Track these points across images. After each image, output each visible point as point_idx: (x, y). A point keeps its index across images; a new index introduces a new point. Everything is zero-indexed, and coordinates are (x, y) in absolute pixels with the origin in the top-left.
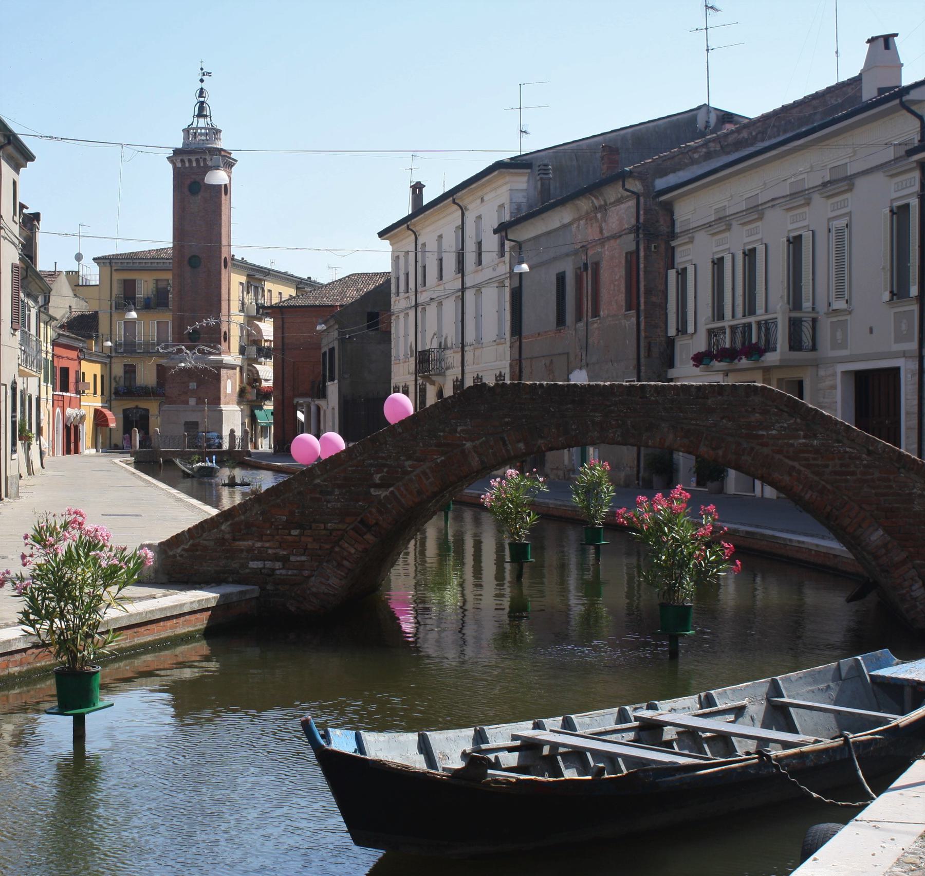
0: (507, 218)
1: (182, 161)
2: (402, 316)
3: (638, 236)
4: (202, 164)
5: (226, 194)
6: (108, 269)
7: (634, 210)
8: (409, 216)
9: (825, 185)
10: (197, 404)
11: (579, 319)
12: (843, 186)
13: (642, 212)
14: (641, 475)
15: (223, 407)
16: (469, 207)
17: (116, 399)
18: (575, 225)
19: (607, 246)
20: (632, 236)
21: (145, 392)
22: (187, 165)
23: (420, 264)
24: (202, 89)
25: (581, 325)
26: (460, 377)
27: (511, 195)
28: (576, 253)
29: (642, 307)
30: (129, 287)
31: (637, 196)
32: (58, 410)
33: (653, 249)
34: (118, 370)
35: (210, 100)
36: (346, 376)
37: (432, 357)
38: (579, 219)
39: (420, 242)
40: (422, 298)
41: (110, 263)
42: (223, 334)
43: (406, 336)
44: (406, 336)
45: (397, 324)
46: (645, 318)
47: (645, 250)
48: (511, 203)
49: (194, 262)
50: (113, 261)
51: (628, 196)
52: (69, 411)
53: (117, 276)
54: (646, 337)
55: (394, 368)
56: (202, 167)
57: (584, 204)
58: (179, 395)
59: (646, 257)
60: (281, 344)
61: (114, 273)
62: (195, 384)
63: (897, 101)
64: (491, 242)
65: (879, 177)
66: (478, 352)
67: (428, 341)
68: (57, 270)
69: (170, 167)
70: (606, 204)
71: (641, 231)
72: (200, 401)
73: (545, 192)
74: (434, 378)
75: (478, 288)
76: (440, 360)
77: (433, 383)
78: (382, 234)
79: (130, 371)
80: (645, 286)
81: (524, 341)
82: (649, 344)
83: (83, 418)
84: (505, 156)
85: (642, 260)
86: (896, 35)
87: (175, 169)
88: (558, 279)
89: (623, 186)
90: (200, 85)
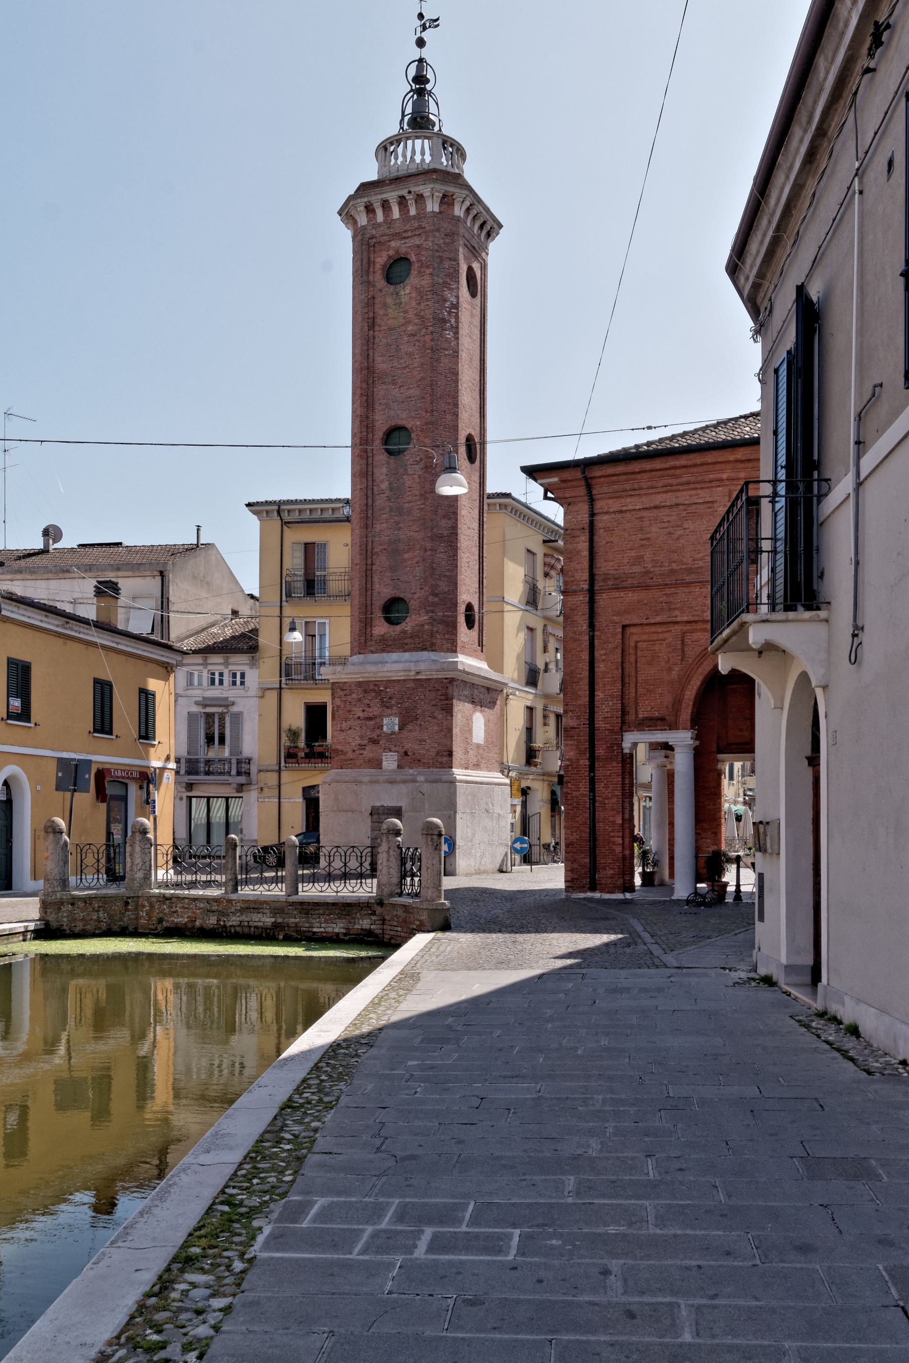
1: (370, 209)
4: (413, 211)
5: (473, 294)
10: (399, 767)
15: (459, 773)
22: (380, 217)
24: (421, 61)
35: (438, 87)
41: (279, 512)
42: (462, 608)
56: (414, 217)
58: (362, 747)
60: (586, 576)
61: (285, 527)
62: (396, 720)
68: (202, 541)
72: (407, 759)
90: (416, 53)
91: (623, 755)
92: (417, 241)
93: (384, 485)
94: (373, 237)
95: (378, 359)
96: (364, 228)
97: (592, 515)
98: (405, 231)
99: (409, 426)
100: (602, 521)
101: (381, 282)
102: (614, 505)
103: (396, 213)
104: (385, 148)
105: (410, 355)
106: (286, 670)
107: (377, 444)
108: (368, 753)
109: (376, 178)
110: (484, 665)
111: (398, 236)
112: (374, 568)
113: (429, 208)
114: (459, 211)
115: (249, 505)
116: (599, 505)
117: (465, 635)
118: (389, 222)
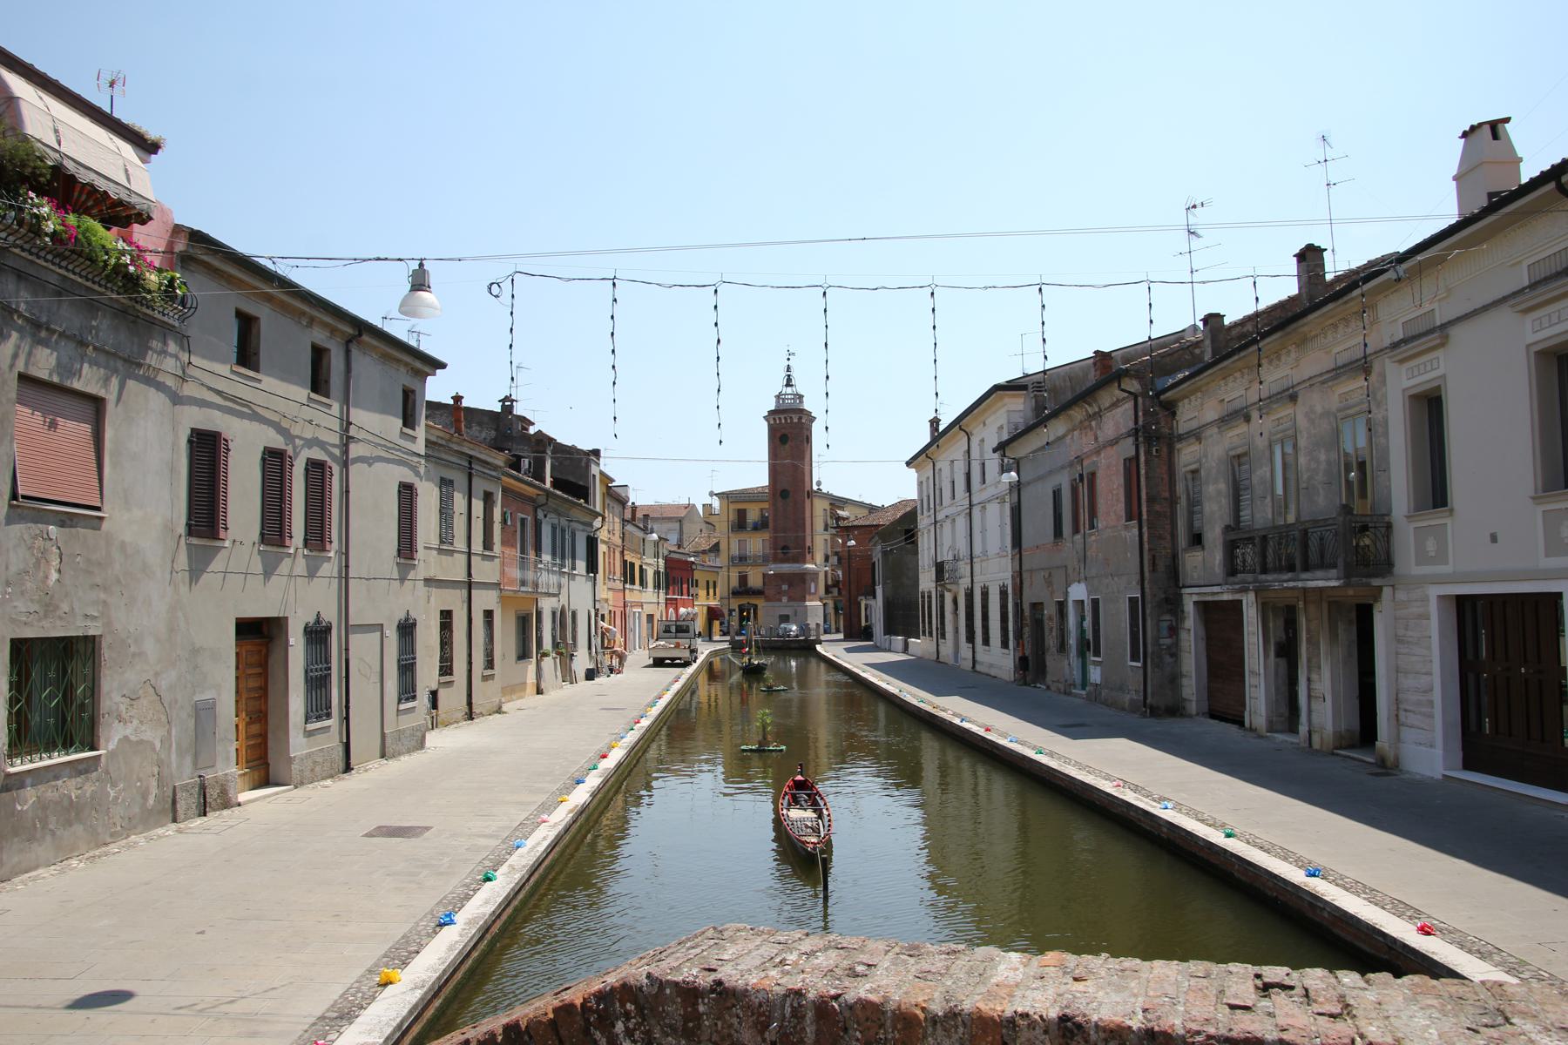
0: (1005, 437)
1: (774, 419)
2: (925, 532)
3: (1137, 440)
4: (789, 421)
7: (1132, 412)
8: (929, 443)
9: (1395, 346)
11: (1076, 530)
12: (1434, 339)
13: (1140, 414)
14: (1148, 701)
16: (974, 432)
18: (1070, 437)
19: (1103, 455)
20: (1131, 440)
21: (758, 593)
22: (778, 422)
23: (937, 487)
25: (1078, 537)
26: (970, 586)
27: (1008, 416)
28: (1071, 464)
29: (1145, 517)
30: (742, 514)
31: (1135, 396)
32: (671, 610)
33: (1154, 453)
35: (794, 374)
36: (888, 581)
37: (947, 567)
38: (1074, 430)
39: (937, 468)
40: (940, 516)
43: (929, 548)
44: (929, 548)
45: (923, 538)
46: (1148, 528)
47: (1145, 455)
48: (1009, 423)
49: (784, 494)
51: (1124, 399)
52: (682, 610)
53: (732, 507)
54: (1150, 550)
55: (921, 576)
57: (1077, 414)
59: (1147, 462)
63: (1552, 185)
64: (993, 462)
65: (1505, 315)
66: (984, 564)
67: (945, 554)
69: (766, 423)
70: (1100, 410)
71: (1140, 434)
72: (791, 599)
73: (1039, 407)
74: (948, 586)
75: (983, 505)
76: (955, 570)
77: (949, 591)
78: (908, 464)
79: (743, 579)
80: (1147, 493)
81: (1023, 553)
82: (1154, 557)
83: (696, 615)
84: (1002, 380)
85: (1142, 466)
86: (1507, 120)
87: (769, 425)
88: (1054, 492)
89: (1119, 386)
90: (787, 363)
101: (778, 442)
103: (783, 421)
104: (778, 397)
106: (732, 559)
108: (777, 597)
109: (773, 408)
110: (814, 566)
111: (784, 428)
114: (803, 421)
117: (808, 557)
118: (780, 423)
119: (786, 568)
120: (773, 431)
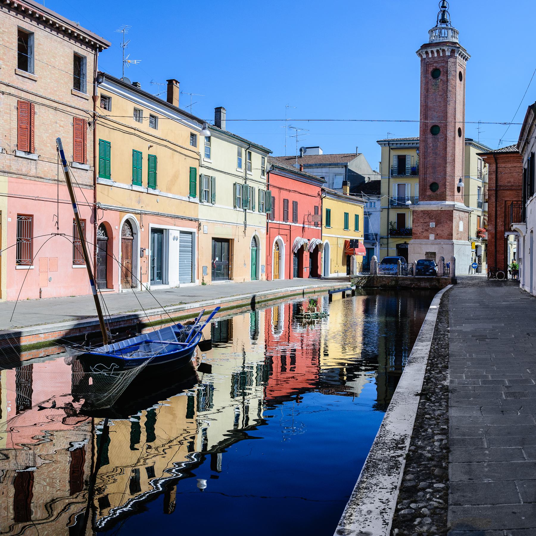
1: (427, 53)
4: (441, 55)
5: (461, 80)
6: (387, 148)
10: (435, 239)
15: (454, 241)
17: (391, 238)
22: (430, 56)
30: (402, 160)
34: (393, 218)
35: (451, 9)
41: (389, 144)
50: (390, 142)
53: (395, 153)
61: (391, 150)
62: (434, 223)
69: (419, 59)
72: (438, 236)
79: (401, 218)
87: (423, 60)
91: (505, 238)
92: (443, 64)
93: (431, 145)
94: (428, 62)
95: (429, 103)
96: (425, 59)
97: (497, 168)
98: (439, 61)
99: (439, 126)
100: (500, 170)
101: (431, 77)
102: (503, 165)
104: (431, 31)
105: (440, 102)
106: (391, 203)
107: (429, 131)
108: (425, 234)
112: (427, 172)
113: (447, 54)
115: (378, 142)
116: (498, 165)
118: (433, 57)
119: (433, 206)
120: (425, 64)
